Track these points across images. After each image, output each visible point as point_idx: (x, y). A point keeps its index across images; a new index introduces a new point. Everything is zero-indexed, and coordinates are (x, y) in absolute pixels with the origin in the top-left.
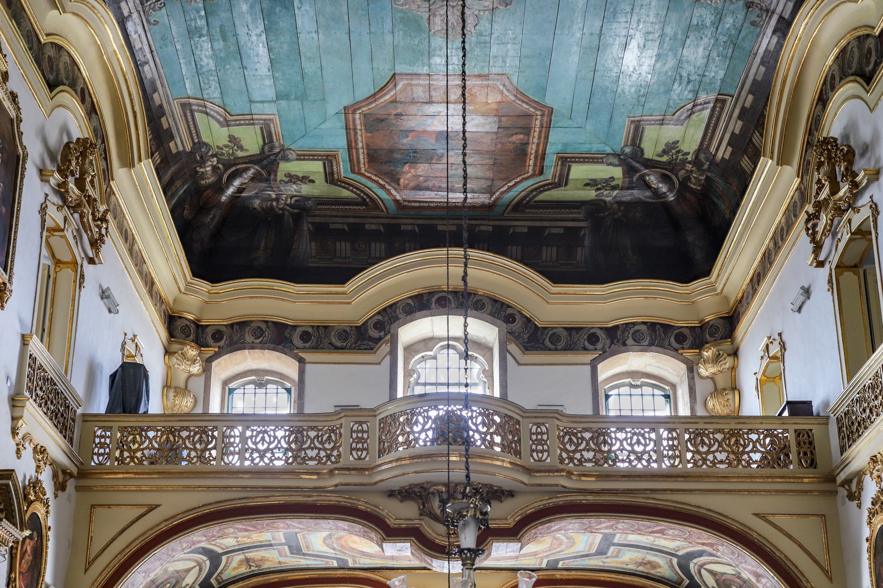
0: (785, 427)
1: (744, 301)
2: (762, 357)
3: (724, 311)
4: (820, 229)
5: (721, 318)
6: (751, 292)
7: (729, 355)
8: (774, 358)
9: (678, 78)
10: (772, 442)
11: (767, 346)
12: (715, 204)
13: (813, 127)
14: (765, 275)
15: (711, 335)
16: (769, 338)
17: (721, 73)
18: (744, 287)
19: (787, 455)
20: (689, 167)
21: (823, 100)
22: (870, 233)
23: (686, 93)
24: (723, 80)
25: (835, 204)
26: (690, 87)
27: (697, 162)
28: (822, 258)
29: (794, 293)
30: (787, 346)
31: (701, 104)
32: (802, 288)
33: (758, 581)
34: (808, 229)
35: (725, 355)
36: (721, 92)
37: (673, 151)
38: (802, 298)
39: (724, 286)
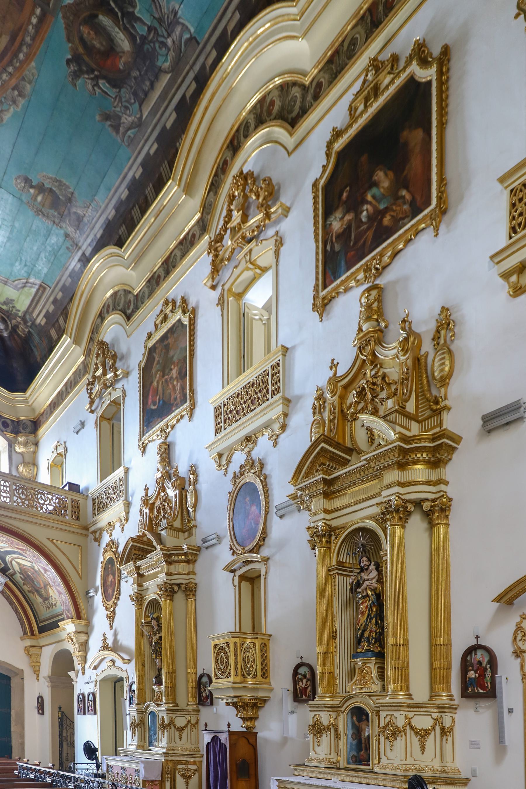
0: (67, 495)
1: (44, 415)
2: (53, 452)
3: (32, 417)
4: (94, 392)
5: (30, 420)
6: (49, 412)
7: (33, 444)
8: (60, 454)
9: (19, 259)
10: (59, 502)
11: (57, 447)
12: (32, 350)
13: (94, 330)
14: (59, 405)
15: (24, 429)
16: (58, 442)
17: (45, 270)
18: (45, 407)
19: (66, 511)
20: (19, 320)
21: (101, 317)
22: (120, 405)
23: (23, 271)
24: (46, 275)
25: (104, 381)
26: (26, 269)
27: (24, 318)
28: (93, 408)
29: (76, 423)
30: (68, 450)
31: (31, 283)
32: (81, 421)
33: (45, 573)
34: (88, 389)
35: (31, 443)
36: (44, 282)
37: (11, 305)
38: (79, 427)
39: (34, 402)
